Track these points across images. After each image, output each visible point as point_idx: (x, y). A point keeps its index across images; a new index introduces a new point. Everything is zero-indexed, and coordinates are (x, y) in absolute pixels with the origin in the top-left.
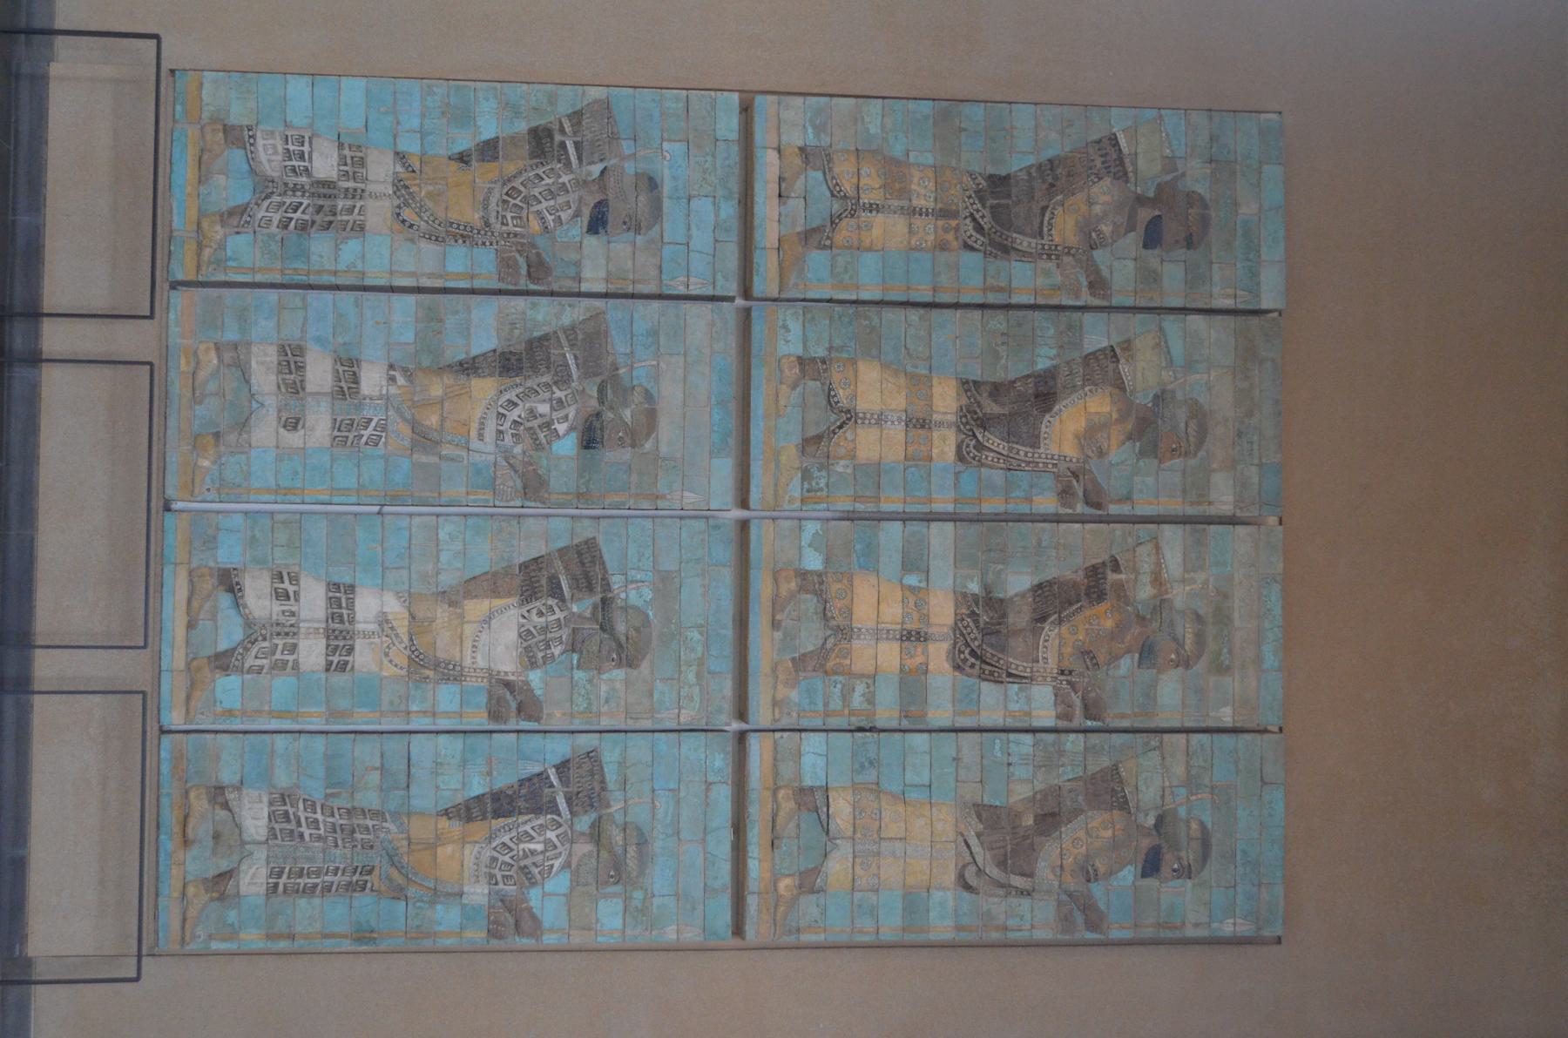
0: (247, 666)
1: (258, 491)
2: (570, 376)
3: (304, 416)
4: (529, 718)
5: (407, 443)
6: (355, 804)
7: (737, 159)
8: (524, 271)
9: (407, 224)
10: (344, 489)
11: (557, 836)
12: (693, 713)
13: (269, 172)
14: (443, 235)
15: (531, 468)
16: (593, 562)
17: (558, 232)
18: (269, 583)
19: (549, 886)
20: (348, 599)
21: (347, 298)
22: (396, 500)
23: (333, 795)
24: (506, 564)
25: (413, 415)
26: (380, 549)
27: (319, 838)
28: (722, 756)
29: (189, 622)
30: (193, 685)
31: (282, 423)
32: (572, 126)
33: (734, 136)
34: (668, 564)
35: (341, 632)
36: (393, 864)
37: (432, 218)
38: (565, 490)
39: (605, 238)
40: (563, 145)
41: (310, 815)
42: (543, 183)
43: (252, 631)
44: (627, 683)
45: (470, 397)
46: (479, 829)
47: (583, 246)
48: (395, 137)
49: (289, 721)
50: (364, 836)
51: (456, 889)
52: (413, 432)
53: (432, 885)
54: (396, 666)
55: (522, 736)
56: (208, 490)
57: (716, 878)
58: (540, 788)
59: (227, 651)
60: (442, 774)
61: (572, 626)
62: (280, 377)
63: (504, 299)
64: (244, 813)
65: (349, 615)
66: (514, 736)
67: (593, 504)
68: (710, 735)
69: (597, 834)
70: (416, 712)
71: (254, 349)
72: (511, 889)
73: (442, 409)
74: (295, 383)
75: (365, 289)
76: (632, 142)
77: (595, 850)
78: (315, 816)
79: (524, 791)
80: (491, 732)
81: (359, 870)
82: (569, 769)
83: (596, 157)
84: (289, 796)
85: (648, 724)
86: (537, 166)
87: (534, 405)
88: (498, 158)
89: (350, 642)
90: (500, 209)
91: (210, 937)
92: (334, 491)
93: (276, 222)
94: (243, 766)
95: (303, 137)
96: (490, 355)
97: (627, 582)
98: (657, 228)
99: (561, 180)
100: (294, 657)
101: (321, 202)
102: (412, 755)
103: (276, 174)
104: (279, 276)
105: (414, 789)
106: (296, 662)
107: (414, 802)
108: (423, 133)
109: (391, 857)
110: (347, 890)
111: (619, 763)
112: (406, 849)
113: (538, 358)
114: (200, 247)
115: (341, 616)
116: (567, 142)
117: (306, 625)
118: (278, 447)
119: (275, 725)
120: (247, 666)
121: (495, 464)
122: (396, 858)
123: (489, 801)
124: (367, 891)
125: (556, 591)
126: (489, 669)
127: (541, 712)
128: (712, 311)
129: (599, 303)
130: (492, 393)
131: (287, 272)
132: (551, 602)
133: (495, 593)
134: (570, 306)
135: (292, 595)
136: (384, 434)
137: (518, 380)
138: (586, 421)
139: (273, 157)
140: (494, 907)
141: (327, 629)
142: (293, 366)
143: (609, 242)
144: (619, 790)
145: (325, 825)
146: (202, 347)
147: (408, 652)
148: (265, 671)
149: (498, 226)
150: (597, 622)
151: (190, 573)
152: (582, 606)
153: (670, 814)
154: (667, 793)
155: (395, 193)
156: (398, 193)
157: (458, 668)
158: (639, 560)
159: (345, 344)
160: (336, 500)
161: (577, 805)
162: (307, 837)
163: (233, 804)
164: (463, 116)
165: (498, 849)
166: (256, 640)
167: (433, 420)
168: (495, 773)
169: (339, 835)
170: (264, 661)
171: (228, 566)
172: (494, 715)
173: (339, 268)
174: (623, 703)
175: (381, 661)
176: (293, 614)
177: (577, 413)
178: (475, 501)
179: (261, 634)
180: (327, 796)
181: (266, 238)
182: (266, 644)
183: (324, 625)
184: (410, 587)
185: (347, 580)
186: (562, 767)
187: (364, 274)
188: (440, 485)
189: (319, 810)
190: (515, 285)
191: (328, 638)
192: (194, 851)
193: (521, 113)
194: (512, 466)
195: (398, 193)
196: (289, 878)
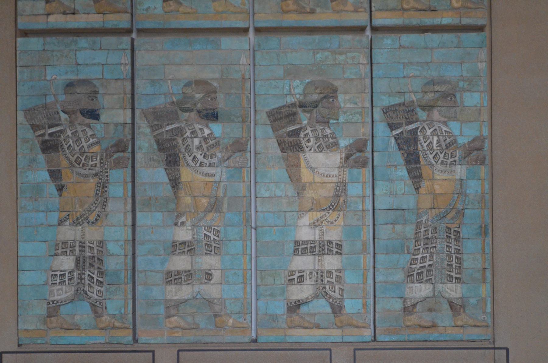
0: (339, 297)
1: (245, 293)
2: (178, 128)
3: (204, 270)
4: (365, 145)
5: (217, 215)
7: (54, 38)
8: (121, 154)
9: (98, 218)
10: (243, 248)
11: (430, 129)
12: (362, 56)
13: (72, 292)
14: (103, 198)
15: (229, 148)
16: (280, 113)
17: (99, 136)
19: (457, 133)
21: (139, 250)
22: (248, 220)
23: (408, 250)
24: (281, 160)
25: (202, 212)
26: (275, 228)
27: (431, 256)
28: (385, 40)
29: (315, 328)
30: (350, 325)
31: (208, 281)
32: (40, 130)
33: (41, 40)
34: (280, 72)
35: (320, 247)
37: (94, 205)
38: (241, 129)
39: (101, 111)
40: (51, 135)
41: (419, 261)
42: (72, 145)
43: (321, 294)
44: (345, 93)
45: (191, 181)
46: (425, 171)
47: (106, 122)
48: (50, 226)
49: (369, 274)
50: (430, 233)
51: (459, 183)
52: (211, 212)
53: (456, 196)
54: (338, 218)
55: (375, 149)
56: (245, 319)
57: (452, 42)
58: (403, 139)
59: (331, 308)
60: (396, 191)
62: (183, 283)
63: (137, 165)
64: (418, 296)
66: (375, 154)
67: (248, 114)
68: (373, 47)
69: (428, 107)
70: (363, 206)
71: (169, 297)
72: (458, 153)
73: (199, 196)
74: (186, 275)
75: (134, 240)
76: (48, 97)
78: (419, 258)
79: (405, 148)
80: (373, 166)
81: (447, 234)
82: (393, 123)
83: (56, 116)
84: (409, 273)
85: (368, 81)
86: (63, 149)
87: (194, 146)
88: (59, 170)
90: (87, 168)
91: (484, 312)
92: (244, 253)
93: (99, 288)
95: (52, 275)
96: (167, 171)
97: (290, 94)
98: (95, 82)
99: (70, 135)
100: (334, 272)
101: (88, 265)
102: (386, 208)
103: (73, 289)
104: (129, 286)
105: (405, 207)
106: (337, 271)
107: (411, 207)
108: (48, 211)
110: (459, 241)
111: (390, 96)
112: (437, 210)
113: (169, 145)
114: (114, 328)
115: (311, 247)
116: (49, 132)
117: (317, 266)
118: (221, 284)
119: (370, 281)
120: (339, 297)
121: (227, 167)
122: (442, 215)
123: (410, 166)
125: (296, 133)
126: (339, 168)
127: (361, 139)
128: (140, 50)
129: (138, 113)
130: (189, 169)
131: (126, 281)
132: (302, 135)
133: (297, 166)
134: (139, 129)
136: (213, 227)
137: (181, 156)
138: (203, 118)
139: (64, 290)
141: (319, 255)
142: (178, 277)
143: (104, 108)
144: (404, 96)
145: (424, 253)
146: (168, 325)
147: (331, 211)
148: (342, 287)
149: (97, 169)
150: (312, 110)
151: (290, 328)
152: (304, 118)
154: (405, 69)
155: (81, 225)
156: (81, 223)
157: (339, 184)
158: (278, 87)
159: (164, 249)
160: (249, 252)
161: (412, 119)
163: (413, 302)
164: (37, 189)
165: (436, 161)
166: (325, 292)
167: (204, 201)
168: (395, 163)
169: (430, 246)
170: (336, 288)
171: (286, 308)
172: (364, 164)
173: (123, 254)
174: (356, 95)
177: (198, 123)
178: (248, 178)
180: (408, 253)
181: (108, 294)
182: (327, 287)
183: (317, 257)
184: (296, 211)
185: (292, 245)
186: (392, 127)
187: (125, 241)
188: (239, 197)
189: (416, 257)
190: (129, 159)
191: (323, 254)
192: (439, 322)
193: (34, 158)
194: (228, 158)
195: (81, 223)
196: (452, 272)
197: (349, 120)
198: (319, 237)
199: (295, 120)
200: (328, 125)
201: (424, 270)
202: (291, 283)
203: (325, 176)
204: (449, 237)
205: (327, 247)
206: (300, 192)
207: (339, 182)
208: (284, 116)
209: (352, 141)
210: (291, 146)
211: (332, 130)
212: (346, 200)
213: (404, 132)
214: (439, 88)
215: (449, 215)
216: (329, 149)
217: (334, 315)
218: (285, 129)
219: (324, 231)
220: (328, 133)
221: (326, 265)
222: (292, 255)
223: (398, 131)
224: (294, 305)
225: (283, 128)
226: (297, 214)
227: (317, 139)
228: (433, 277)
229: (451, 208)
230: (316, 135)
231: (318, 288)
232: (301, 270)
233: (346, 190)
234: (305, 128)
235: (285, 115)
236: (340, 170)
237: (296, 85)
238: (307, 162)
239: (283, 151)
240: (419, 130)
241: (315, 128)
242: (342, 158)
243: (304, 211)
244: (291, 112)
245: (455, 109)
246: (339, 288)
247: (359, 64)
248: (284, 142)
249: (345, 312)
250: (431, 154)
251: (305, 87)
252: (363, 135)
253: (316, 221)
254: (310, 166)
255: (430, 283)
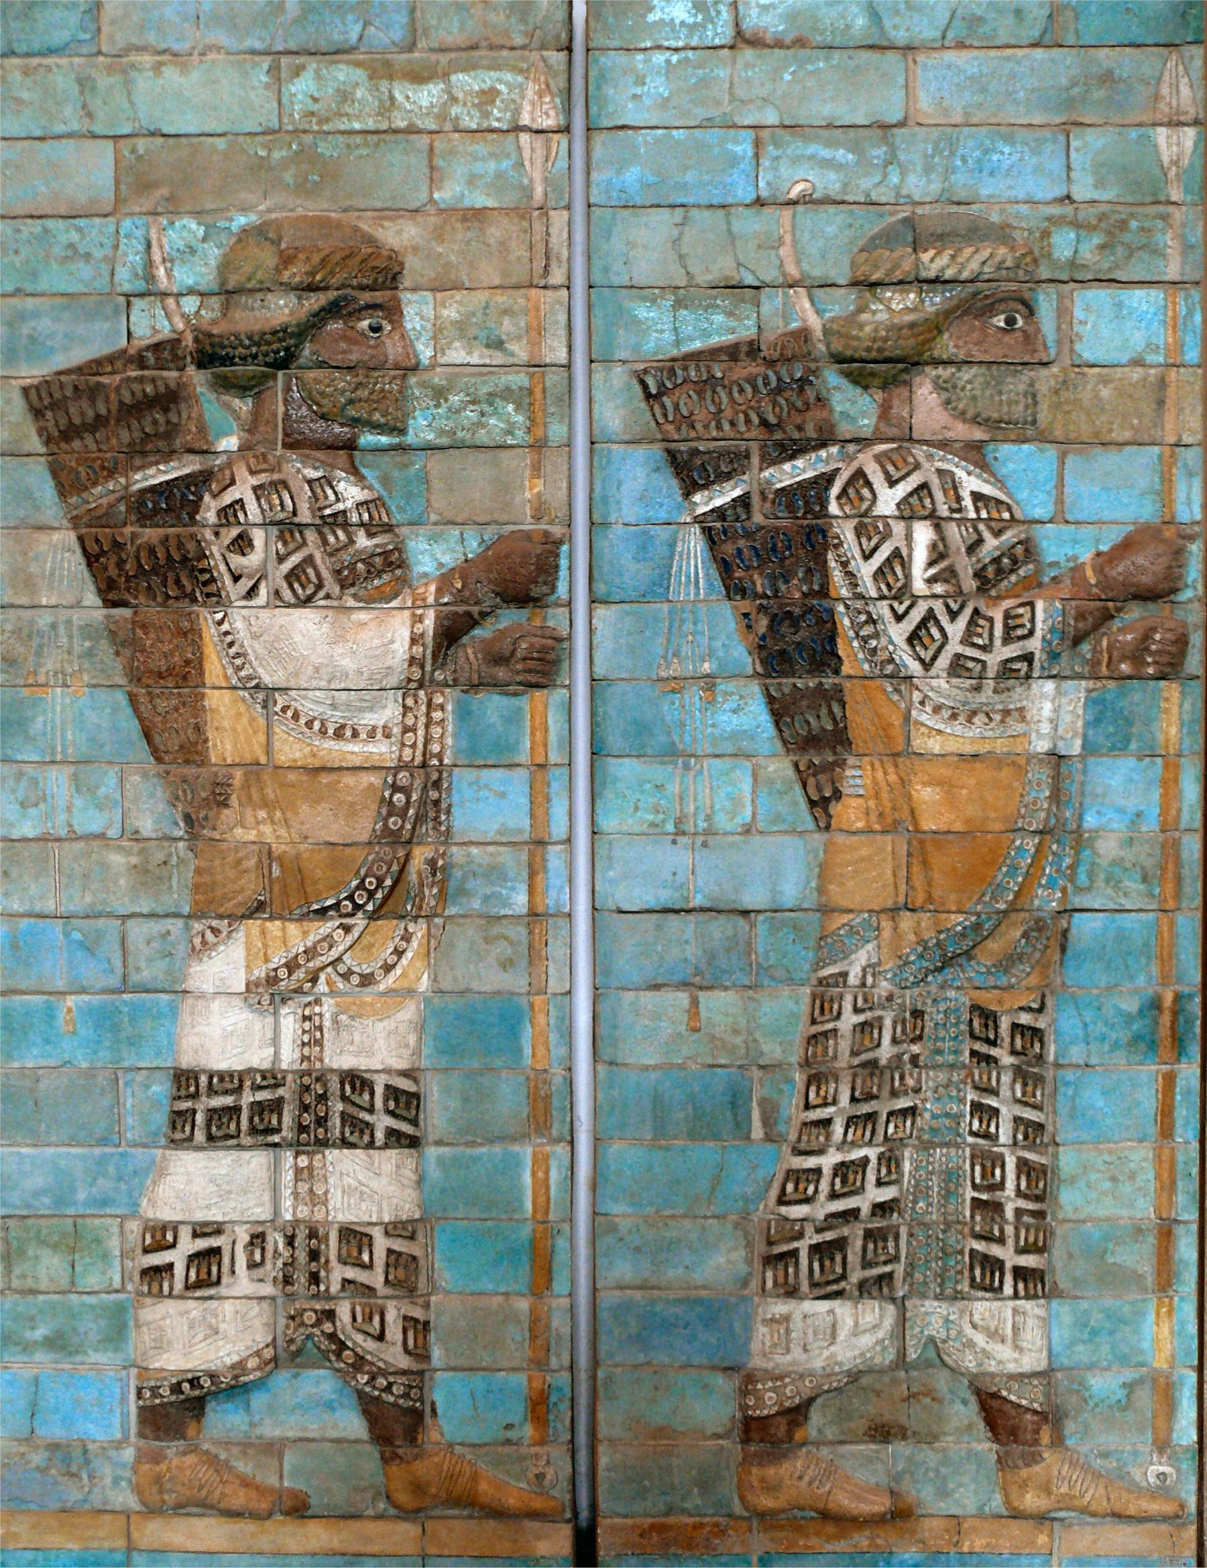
0: (404, 1362)
6: (794, 1059)
11: (892, 483)
18: (171, 1306)
19: (1036, 504)
20: (212, 1091)
27: (890, 1160)
35: (305, 1108)
36: (968, 954)
41: (824, 1186)
44: (443, 286)
51: (1041, 775)
53: (1031, 844)
54: (399, 953)
58: (748, 535)
59: (366, 1413)
60: (708, 818)
61: (279, 451)
64: (818, 1364)
65: (257, 1088)
72: (1044, 614)
77: (931, 372)
78: (827, 1171)
79: (760, 584)
82: (695, 452)
84: (770, 1243)
89: (334, 1084)
94: (686, 1366)
100: (377, 1233)
102: (652, 903)
105: (753, 898)
106: (394, 1229)
109: (947, 962)
110: (1039, 1080)
111: (678, 304)
112: (925, 919)
115: (259, 1108)
117: (287, 1202)
120: (404, 1362)
123: (787, 682)
124: (1041, 1025)
126: (406, 688)
127: (527, 536)
135: (202, 1244)
140: (1095, 663)
147: (359, 921)
148: (418, 1313)
150: (265, 377)
153: (826, 153)
154: (765, 162)
157: (403, 778)
161: (800, 428)
162: (887, 1194)
163: (792, 1394)
165: (927, 655)
166: (332, 1337)
168: (706, 667)
169: (883, 1107)
170: (391, 1316)
174: (501, 299)
175: (389, 992)
176: (258, 1239)
179: (318, 1323)
180: (769, 1138)
182: (343, 1311)
183: (288, 1157)
184: (177, 915)
185: (161, 1089)
189: (811, 1162)
191: (323, 1144)
196: (1001, 1241)
197: (460, 434)
198: (297, 1055)
199: (172, 431)
200: (351, 457)
201: (855, 1233)
202: (155, 1289)
203: (331, 732)
204: (990, 1060)
205: (340, 1106)
206: (201, 815)
207: (402, 766)
208: (114, 407)
209: (475, 544)
210: (154, 571)
211: (370, 488)
212: (440, 863)
213: (756, 500)
214: (944, 260)
215: (991, 945)
216: (352, 590)
217: (382, 1454)
218: (123, 480)
219: (327, 1023)
220: (349, 504)
221: (336, 1199)
222: (163, 1141)
223: (724, 495)
224: (173, 1398)
225: (111, 473)
226: (187, 928)
227: (287, 535)
228: (899, 1269)
229: (1002, 906)
230: (282, 516)
231: (293, 1318)
232: (206, 1224)
233: (444, 805)
234: (227, 472)
235: (121, 403)
236: (410, 702)
237: (181, 244)
238: (238, 655)
239: (112, 596)
240: (835, 491)
241: (276, 477)
242: (422, 635)
243: (221, 917)
244: (149, 389)
245: (1027, 375)
246: (405, 1318)
247: (518, 129)
248: (117, 546)
249: (434, 1435)
250: (899, 618)
251: (225, 255)
252: (537, 518)
253: (283, 973)
254: (250, 678)
255: (882, 1297)
